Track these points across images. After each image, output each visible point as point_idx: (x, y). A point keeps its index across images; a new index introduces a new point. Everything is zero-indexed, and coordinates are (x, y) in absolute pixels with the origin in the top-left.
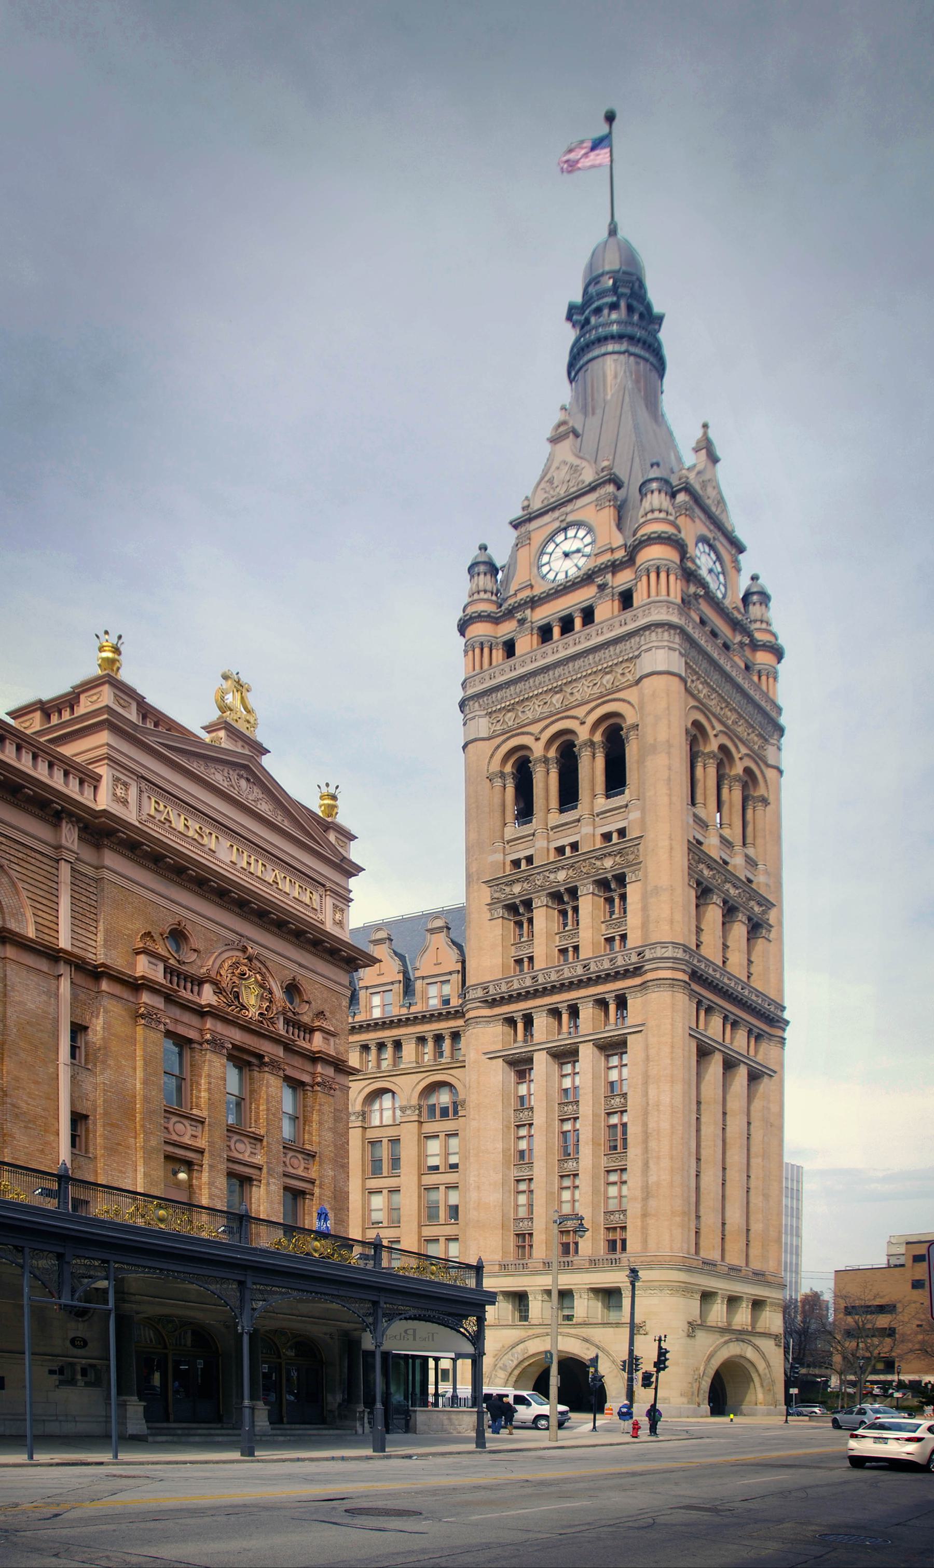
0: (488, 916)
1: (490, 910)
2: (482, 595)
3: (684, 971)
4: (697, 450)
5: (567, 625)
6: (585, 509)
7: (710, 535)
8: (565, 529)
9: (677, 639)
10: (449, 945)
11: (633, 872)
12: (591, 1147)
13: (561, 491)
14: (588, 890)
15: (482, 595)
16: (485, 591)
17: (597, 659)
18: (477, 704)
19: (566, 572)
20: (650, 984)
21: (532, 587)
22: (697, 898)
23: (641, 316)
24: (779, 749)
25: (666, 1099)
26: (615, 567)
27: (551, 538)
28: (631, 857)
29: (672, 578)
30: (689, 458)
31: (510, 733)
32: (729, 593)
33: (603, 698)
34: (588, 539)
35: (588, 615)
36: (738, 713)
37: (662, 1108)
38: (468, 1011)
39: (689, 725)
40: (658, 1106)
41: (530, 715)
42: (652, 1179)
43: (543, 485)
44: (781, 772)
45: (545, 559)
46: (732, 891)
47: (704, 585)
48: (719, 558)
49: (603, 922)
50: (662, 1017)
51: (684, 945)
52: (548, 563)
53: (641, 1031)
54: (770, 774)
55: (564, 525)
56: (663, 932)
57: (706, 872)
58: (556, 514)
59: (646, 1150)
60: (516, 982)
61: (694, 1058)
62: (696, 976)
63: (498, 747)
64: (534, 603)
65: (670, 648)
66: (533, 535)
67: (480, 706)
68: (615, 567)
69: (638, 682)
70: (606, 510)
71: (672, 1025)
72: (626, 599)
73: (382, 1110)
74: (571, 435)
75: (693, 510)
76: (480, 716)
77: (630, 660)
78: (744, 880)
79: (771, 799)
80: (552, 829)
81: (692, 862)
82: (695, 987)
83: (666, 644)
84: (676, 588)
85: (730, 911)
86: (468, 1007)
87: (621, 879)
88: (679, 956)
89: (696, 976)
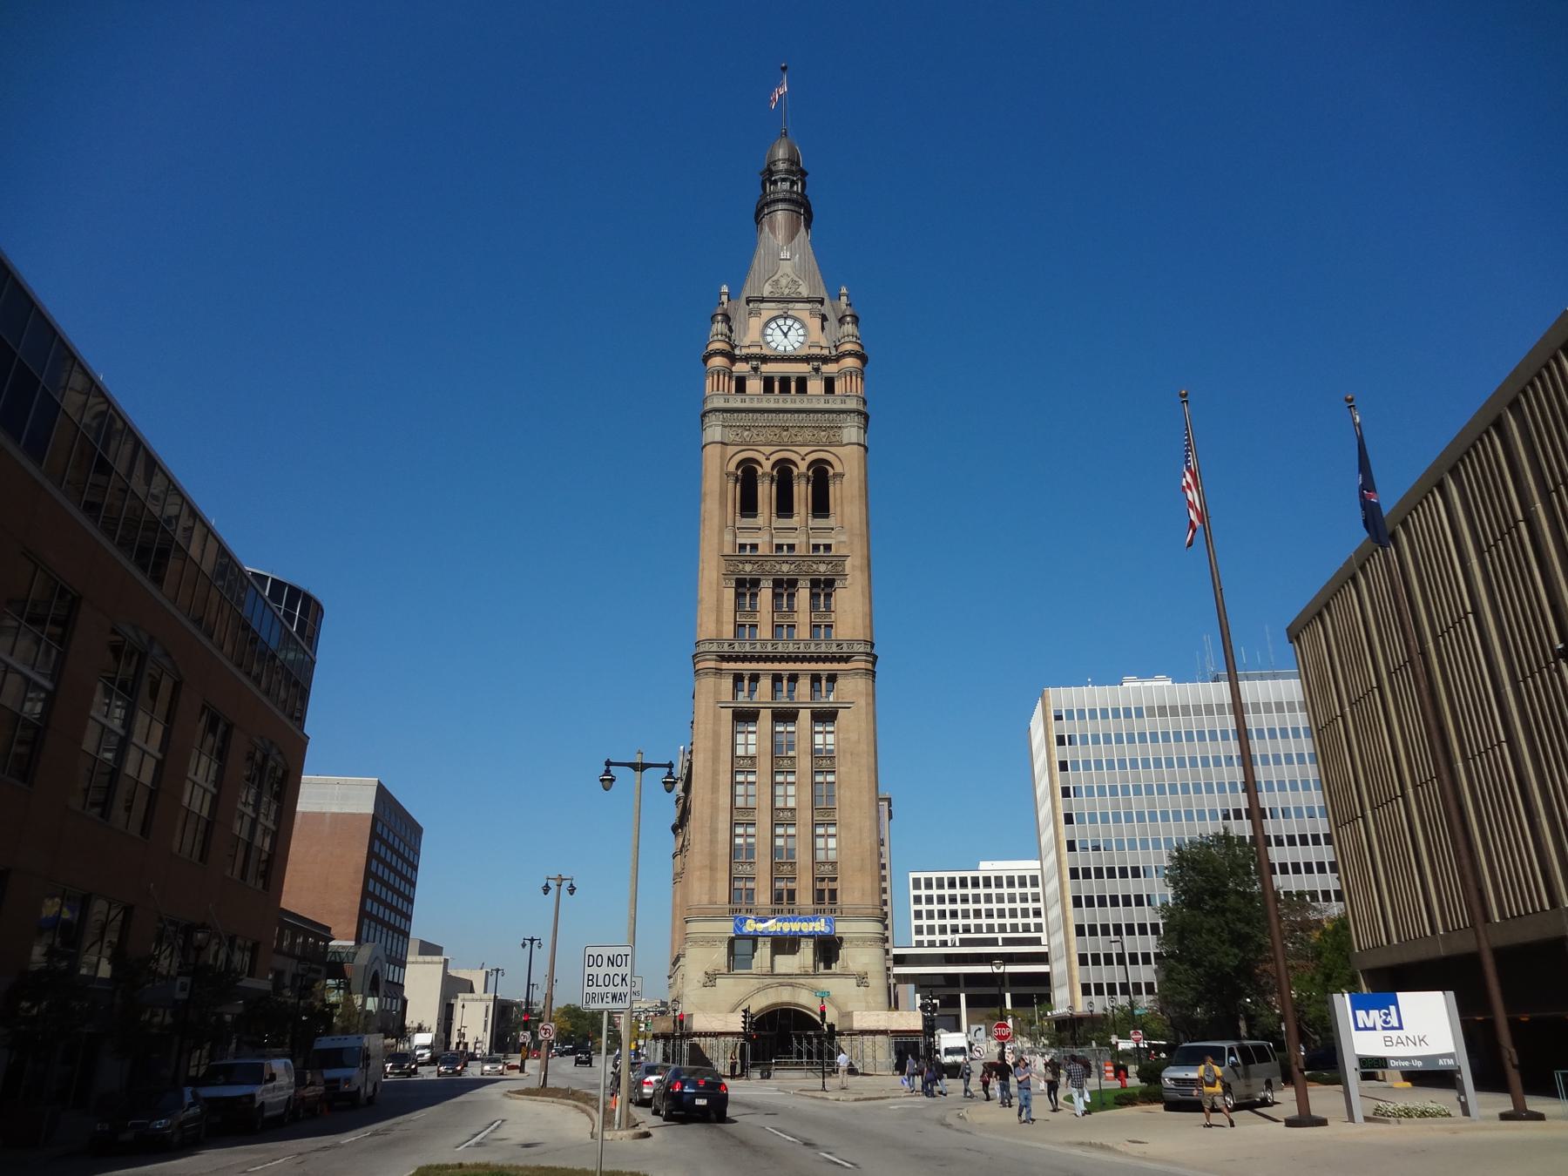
27: (774, 319)
64: (765, 359)
87: (830, 583)
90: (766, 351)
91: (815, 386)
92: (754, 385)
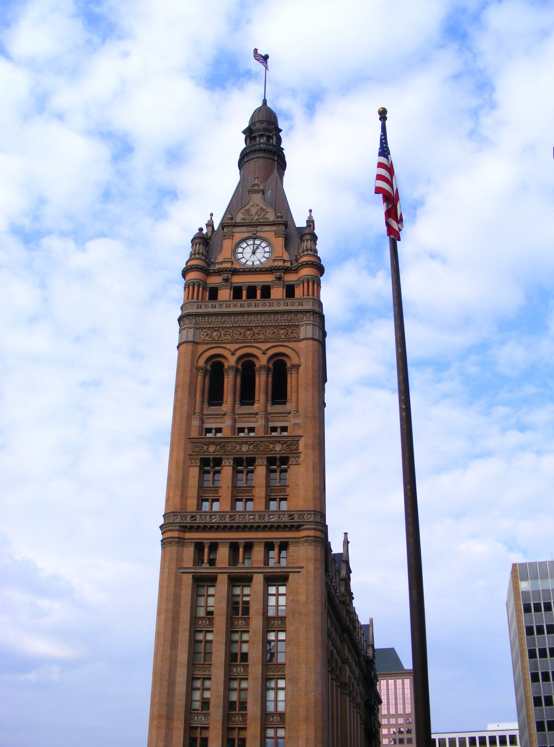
8: (255, 239)
19: (253, 262)
21: (232, 263)
27: (245, 240)
35: (266, 292)
55: (254, 236)
58: (251, 229)
66: (236, 235)
72: (290, 291)
74: (261, 193)
83: (311, 322)
90: (237, 266)
91: (277, 293)
92: (225, 294)
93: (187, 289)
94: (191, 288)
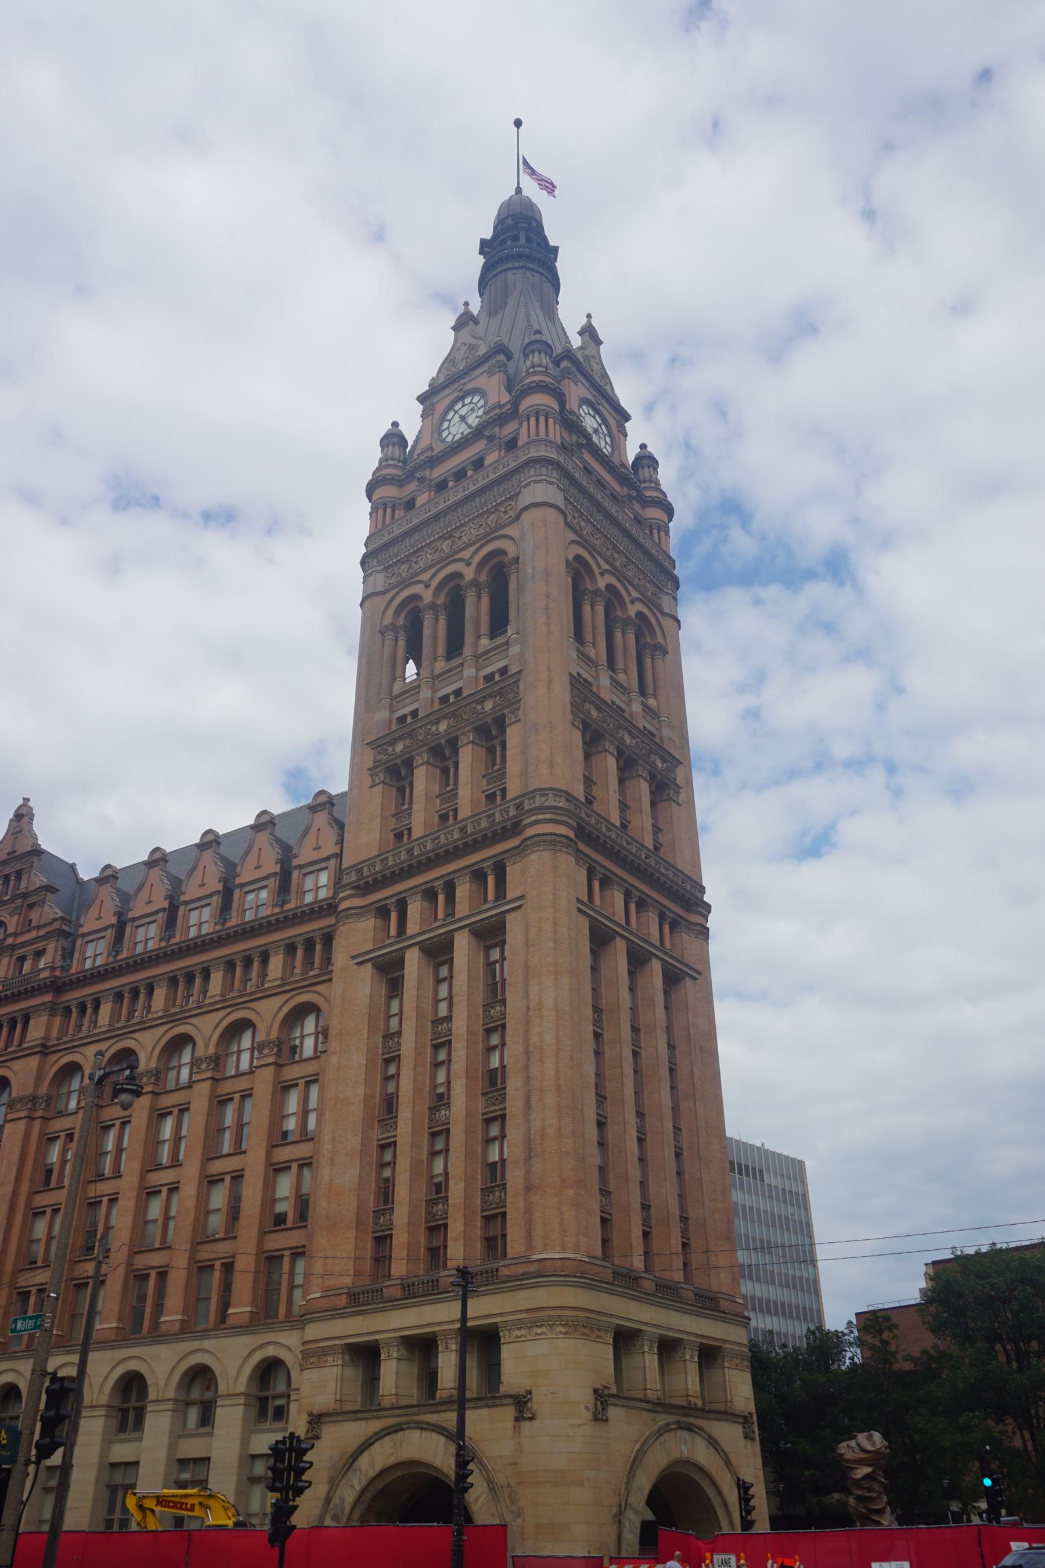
0: (369, 782)
1: (372, 776)
2: (391, 462)
3: (567, 824)
4: (581, 333)
5: (460, 475)
6: (481, 379)
7: (589, 396)
8: (463, 398)
9: (555, 474)
10: (330, 824)
11: (513, 712)
12: (464, 1080)
13: (461, 366)
14: (468, 738)
15: (391, 462)
16: (393, 459)
17: (483, 500)
18: (375, 561)
20: (529, 842)
22: (584, 743)
23: (539, 245)
24: (675, 599)
25: (549, 999)
26: (502, 420)
27: (451, 407)
28: (511, 695)
29: (551, 421)
30: (576, 342)
31: (404, 584)
32: (616, 452)
33: (488, 537)
34: (482, 402)
36: (627, 557)
37: (545, 1013)
38: (339, 902)
39: (571, 559)
40: (539, 1009)
41: (422, 564)
42: (536, 1124)
43: (446, 365)
44: (678, 622)
45: (446, 425)
46: (628, 739)
47: (588, 437)
48: (605, 421)
49: (484, 777)
50: (547, 888)
51: (566, 792)
52: (448, 428)
53: (520, 907)
54: (668, 623)
55: (462, 393)
56: (542, 778)
57: (594, 713)
59: (528, 1079)
60: (390, 859)
61: (585, 947)
62: (584, 833)
63: (392, 599)
64: (433, 462)
65: (548, 482)
66: (436, 406)
67: (378, 561)
68: (502, 420)
69: (518, 517)
70: (496, 376)
71: (554, 894)
72: (511, 444)
73: (239, 1052)
74: (471, 323)
75: (576, 376)
76: (377, 572)
77: (511, 498)
78: (641, 728)
79: (670, 648)
80: (438, 676)
81: (577, 699)
82: (581, 846)
84: (556, 433)
85: (627, 765)
86: (341, 895)
88: (561, 805)
89: (584, 833)
93: (374, 515)
94: (380, 512)
